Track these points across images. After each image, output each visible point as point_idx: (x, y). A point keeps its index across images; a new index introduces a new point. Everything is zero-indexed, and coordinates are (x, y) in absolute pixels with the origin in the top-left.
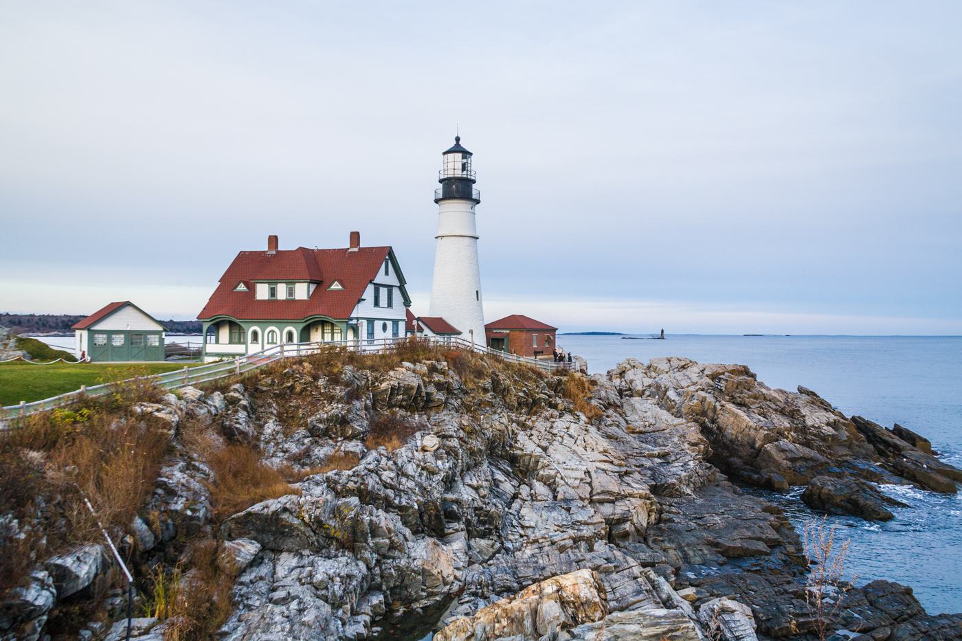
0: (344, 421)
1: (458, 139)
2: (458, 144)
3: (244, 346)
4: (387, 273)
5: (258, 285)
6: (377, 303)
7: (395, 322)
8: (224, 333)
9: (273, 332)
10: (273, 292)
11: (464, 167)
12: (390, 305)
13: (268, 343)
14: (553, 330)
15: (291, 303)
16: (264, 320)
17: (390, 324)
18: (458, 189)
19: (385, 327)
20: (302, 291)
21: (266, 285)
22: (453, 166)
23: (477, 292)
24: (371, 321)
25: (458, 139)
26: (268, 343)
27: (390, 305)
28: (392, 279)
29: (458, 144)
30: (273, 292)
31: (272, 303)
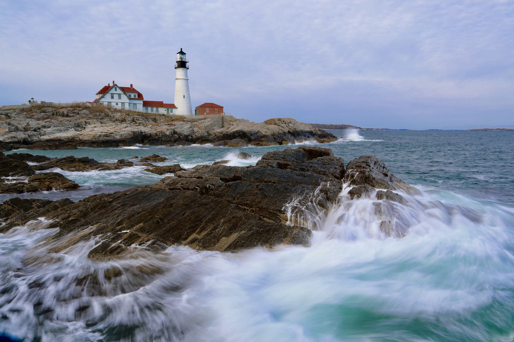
0: (33, 116)
1: (181, 49)
2: (181, 51)
4: (116, 90)
6: (112, 97)
7: (123, 103)
11: (181, 58)
12: (120, 97)
14: (222, 108)
17: (120, 104)
18: (182, 64)
19: (117, 104)
23: (184, 96)
24: (109, 103)
25: (181, 49)
27: (120, 97)
28: (119, 91)
29: (181, 51)
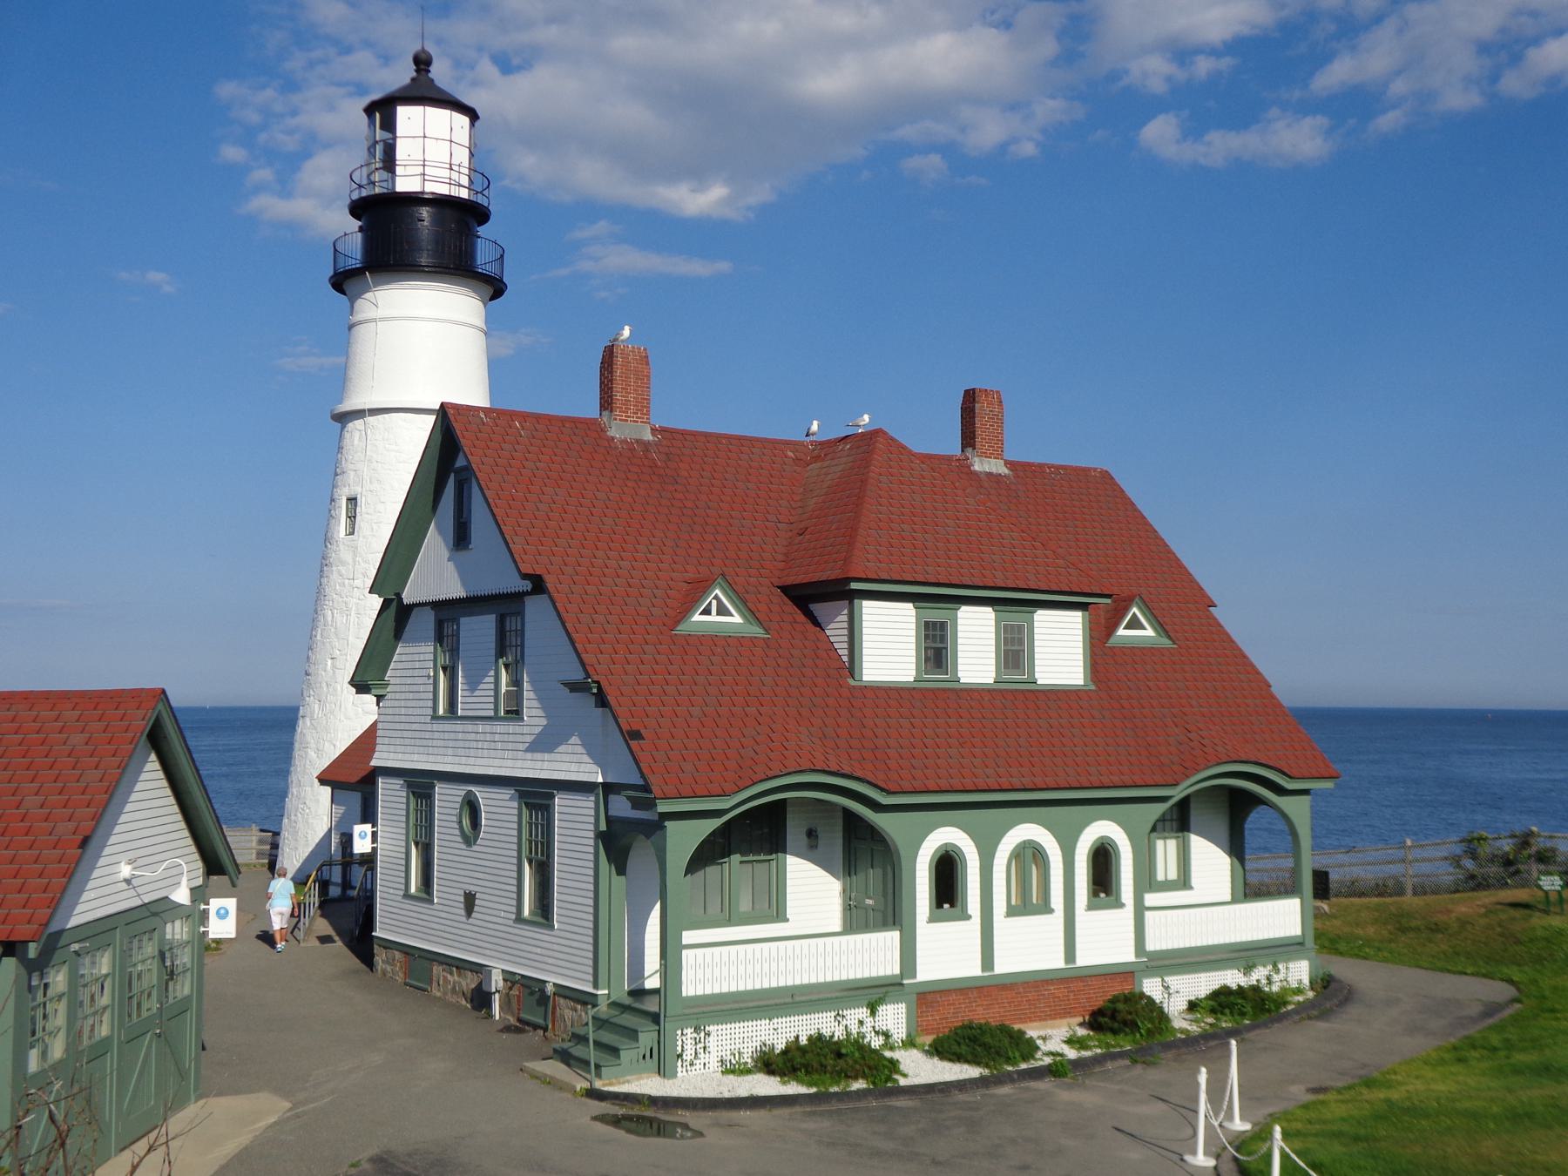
1: (422, 62)
3: (893, 937)
5: (866, 603)
8: (813, 889)
9: (1030, 855)
10: (936, 647)
13: (1012, 912)
15: (1018, 701)
16: (988, 797)
20: (1060, 649)
21: (907, 609)
22: (432, 153)
25: (422, 62)
26: (1012, 912)
30: (936, 647)
31: (934, 700)
